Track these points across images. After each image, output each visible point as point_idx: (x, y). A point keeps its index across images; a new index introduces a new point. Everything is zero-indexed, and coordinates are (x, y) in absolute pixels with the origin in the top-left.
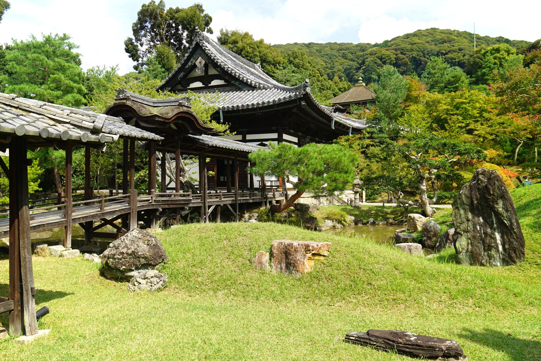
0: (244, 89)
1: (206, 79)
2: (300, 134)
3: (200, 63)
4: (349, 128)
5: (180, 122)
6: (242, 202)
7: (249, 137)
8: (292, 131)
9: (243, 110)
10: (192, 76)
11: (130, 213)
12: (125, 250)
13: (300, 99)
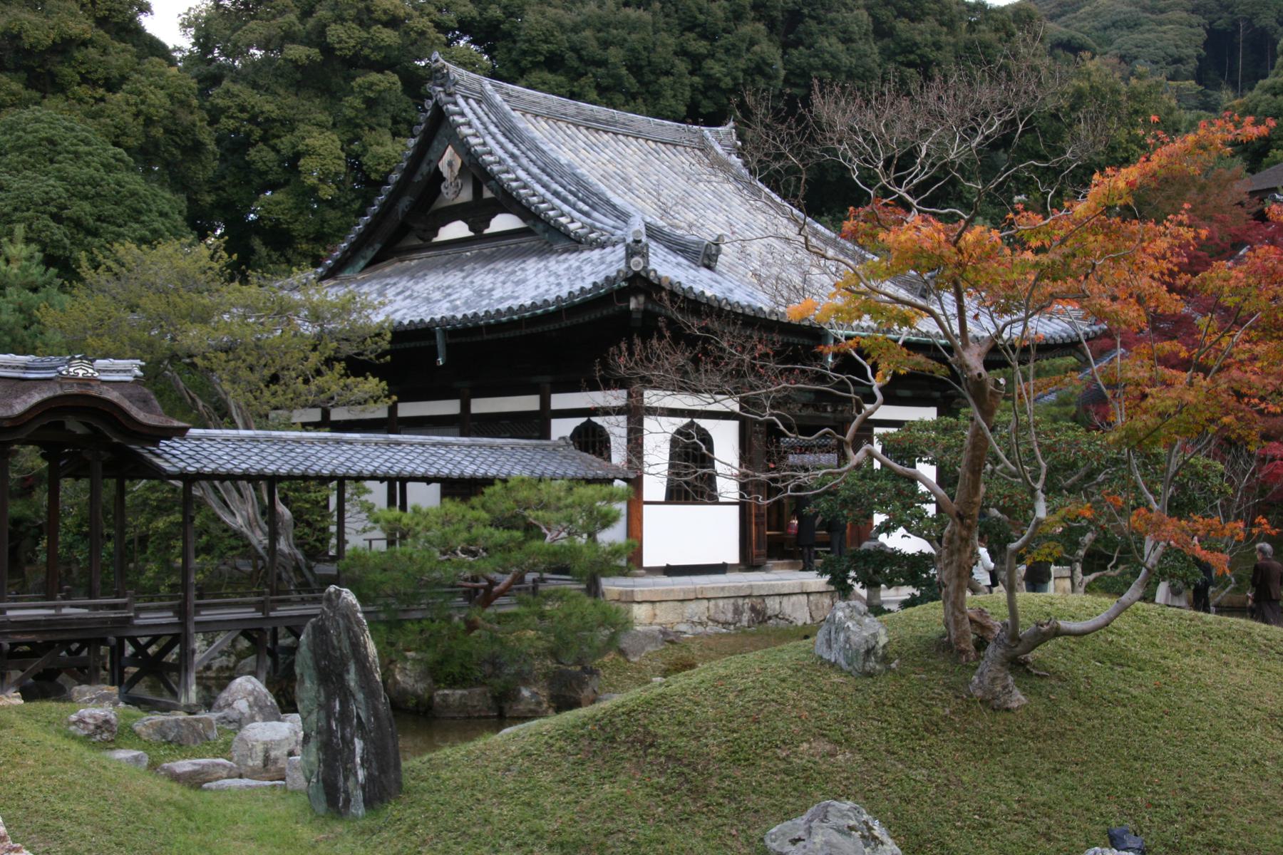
0: (556, 247)
1: (477, 214)
7: (560, 401)
10: (445, 204)
13: (624, 294)
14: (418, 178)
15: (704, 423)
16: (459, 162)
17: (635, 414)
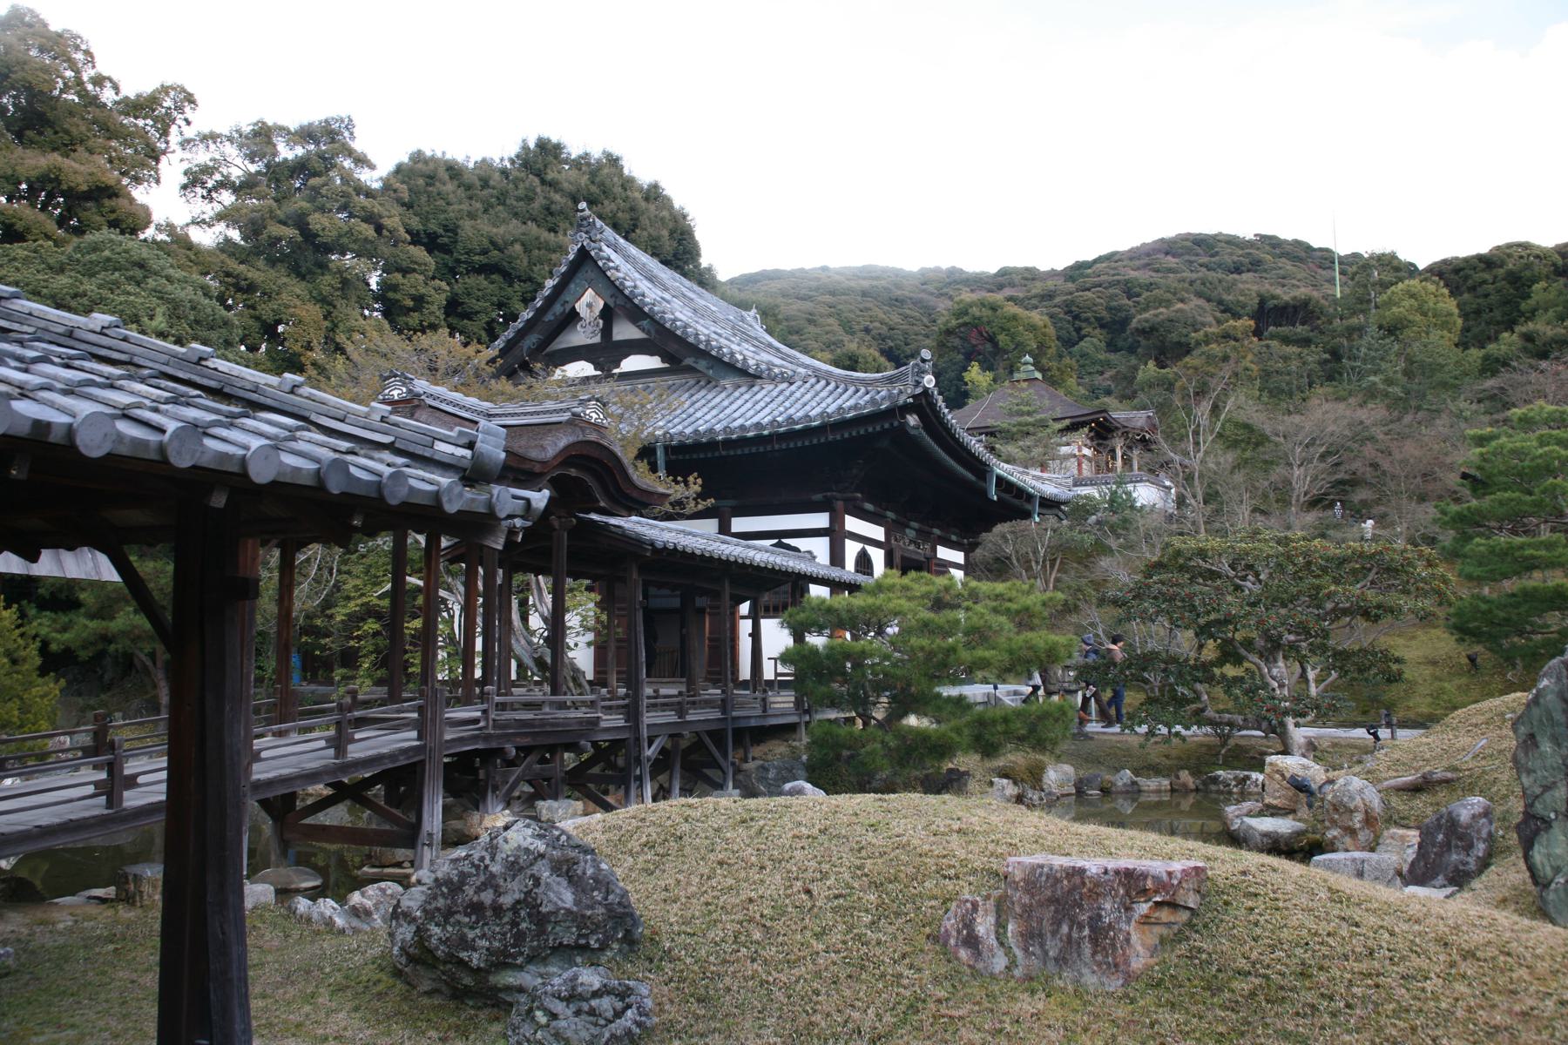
0: (723, 382)
1: (606, 354)
2: (890, 514)
3: (590, 306)
4: (1030, 497)
5: (573, 472)
6: (743, 724)
7: (739, 524)
8: (869, 506)
9: (728, 443)
11: (422, 762)
12: (487, 897)
13: (906, 409)
14: (549, 317)
15: (871, 550)
16: (601, 303)
17: (836, 535)
